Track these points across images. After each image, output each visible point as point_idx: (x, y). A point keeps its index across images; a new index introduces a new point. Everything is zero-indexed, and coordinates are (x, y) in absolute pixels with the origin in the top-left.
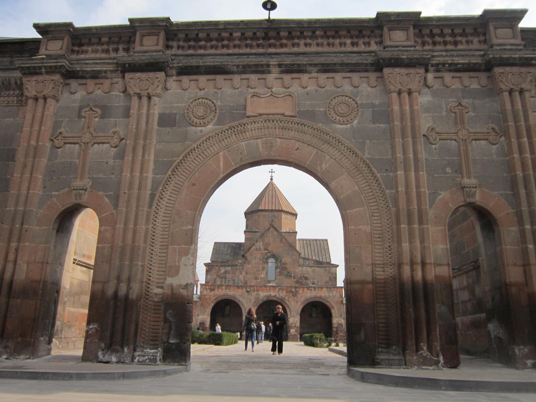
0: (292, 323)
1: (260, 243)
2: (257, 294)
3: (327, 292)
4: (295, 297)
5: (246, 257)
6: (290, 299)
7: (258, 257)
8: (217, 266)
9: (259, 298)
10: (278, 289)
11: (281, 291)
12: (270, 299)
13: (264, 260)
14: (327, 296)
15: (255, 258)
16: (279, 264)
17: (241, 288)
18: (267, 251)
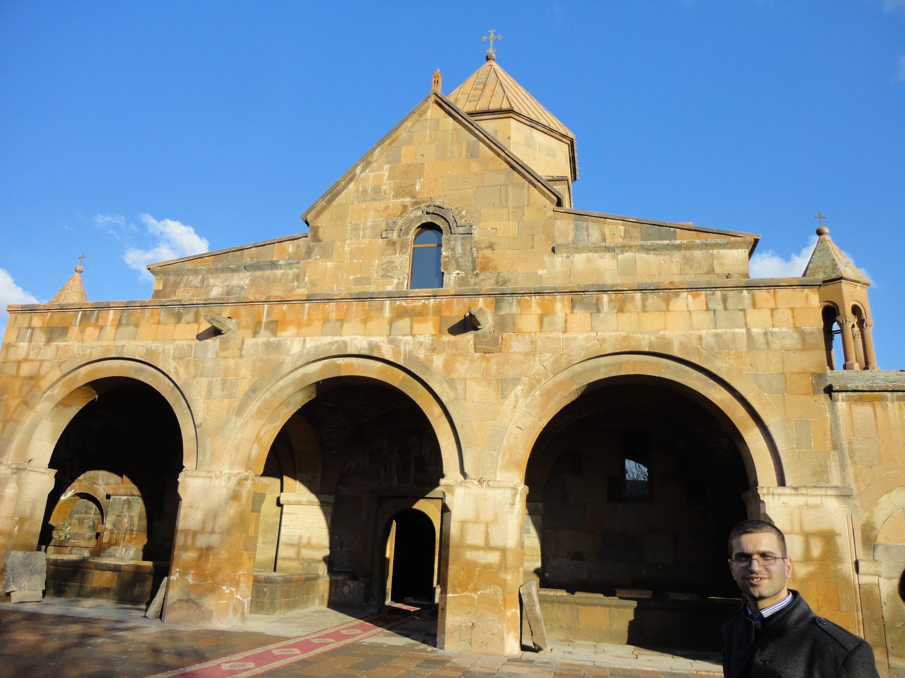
0: (463, 523)
1: (380, 168)
2: (268, 346)
3: (702, 319)
4: (494, 359)
5: (315, 230)
6: (461, 369)
7: (369, 224)
8: (196, 272)
9: (280, 364)
10: (387, 313)
11: (404, 323)
12: (343, 374)
13: (394, 236)
14: (712, 341)
15: (356, 228)
16: (459, 250)
17: (190, 317)
18: (407, 200)
